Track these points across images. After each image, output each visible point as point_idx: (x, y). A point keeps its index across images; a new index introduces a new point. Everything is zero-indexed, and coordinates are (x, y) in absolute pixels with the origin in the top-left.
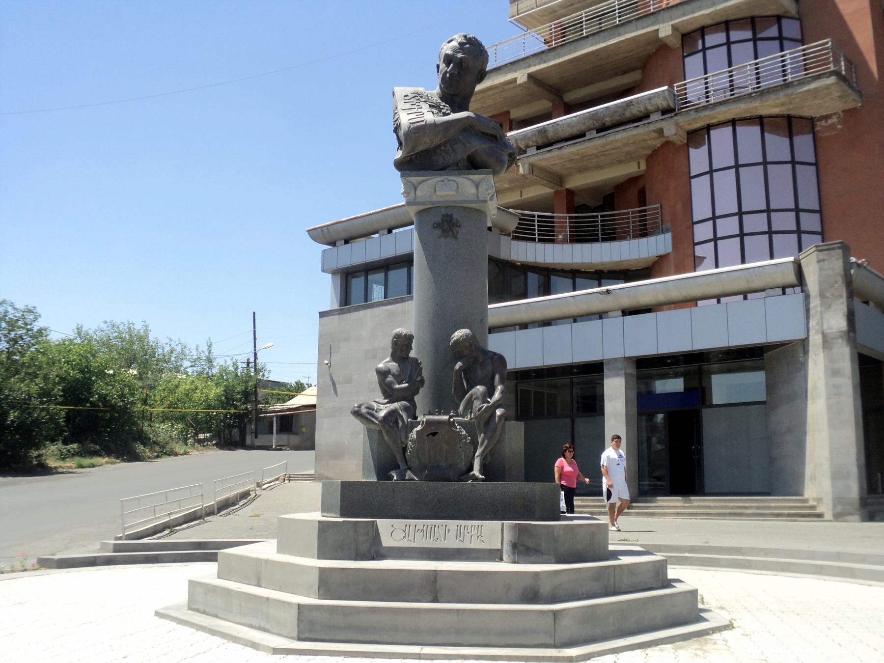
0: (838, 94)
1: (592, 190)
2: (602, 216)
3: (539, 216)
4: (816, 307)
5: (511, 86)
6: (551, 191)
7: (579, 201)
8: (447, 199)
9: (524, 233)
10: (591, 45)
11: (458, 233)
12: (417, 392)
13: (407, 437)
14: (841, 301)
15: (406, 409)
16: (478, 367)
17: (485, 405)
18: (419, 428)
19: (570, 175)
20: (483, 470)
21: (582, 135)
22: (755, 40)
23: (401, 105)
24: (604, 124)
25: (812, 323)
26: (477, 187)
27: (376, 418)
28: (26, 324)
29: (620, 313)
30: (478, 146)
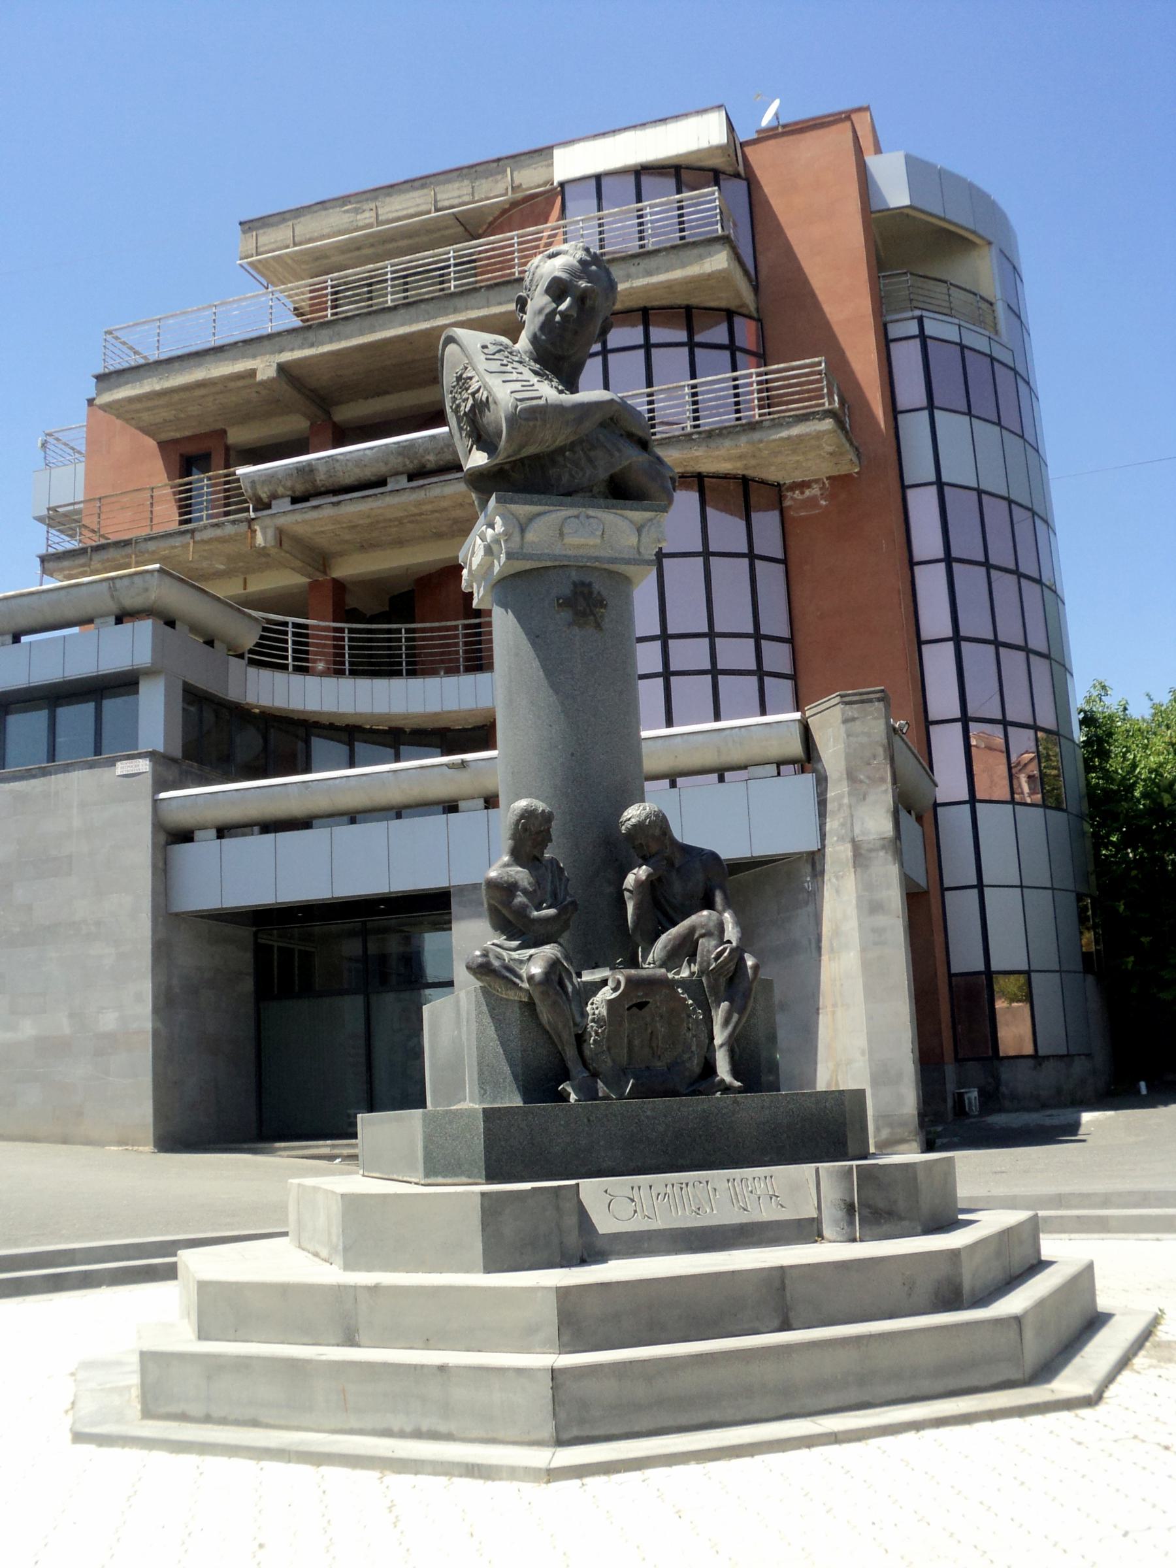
0: (830, 449)
1: (375, 584)
2: (408, 631)
3: (295, 625)
4: (841, 796)
5: (249, 381)
7: (351, 602)
8: (581, 552)
9: (267, 654)
11: (602, 617)
12: (565, 926)
13: (584, 1015)
14: (884, 787)
18: (606, 994)
19: (341, 554)
20: (736, 1073)
21: (381, 482)
22: (692, 345)
24: (424, 467)
25: (831, 825)
26: (639, 530)
27: (531, 978)
29: (481, 802)
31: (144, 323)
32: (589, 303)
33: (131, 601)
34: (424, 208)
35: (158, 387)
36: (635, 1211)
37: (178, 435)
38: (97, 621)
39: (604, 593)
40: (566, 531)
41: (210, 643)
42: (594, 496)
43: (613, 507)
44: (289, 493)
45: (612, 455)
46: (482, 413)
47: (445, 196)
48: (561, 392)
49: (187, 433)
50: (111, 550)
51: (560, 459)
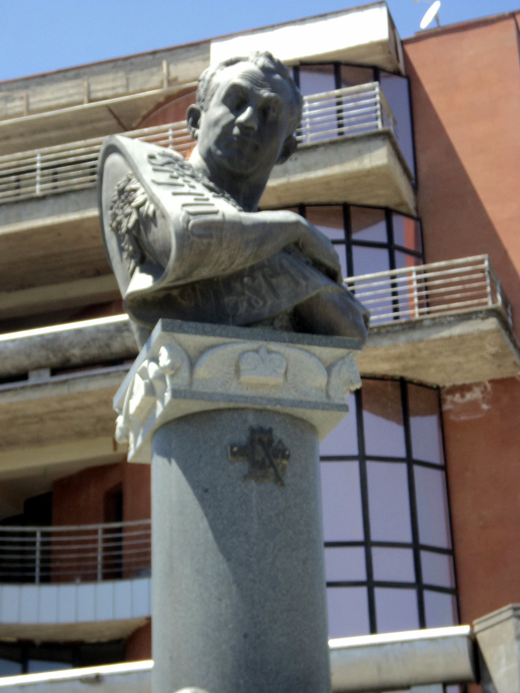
2: (44, 534)
8: (261, 392)
10: (51, 214)
11: (284, 468)
24: (68, 360)
26: (329, 369)
32: (272, 115)
34: (76, 98)
39: (287, 442)
40: (243, 367)
43: (298, 342)
45: (297, 284)
46: (147, 229)
47: (99, 87)
48: (240, 211)
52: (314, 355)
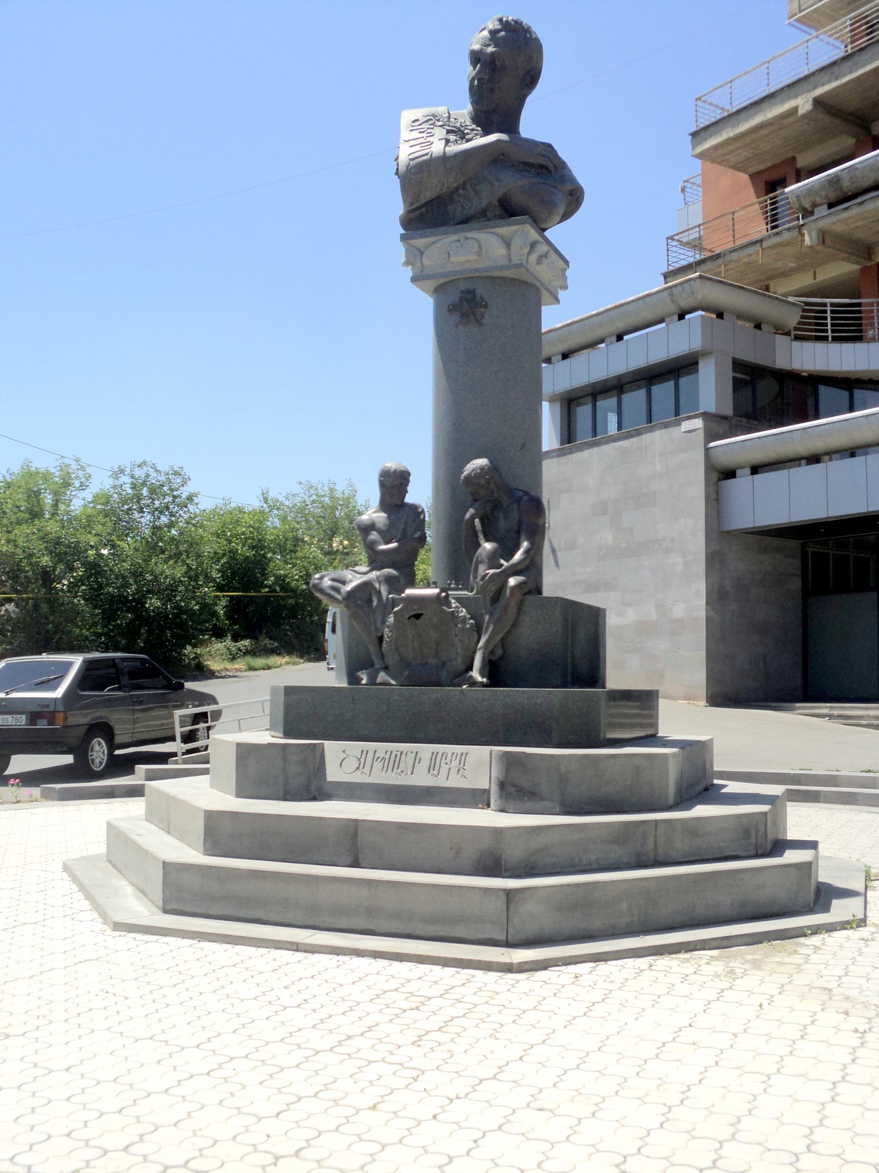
3: (832, 305)
5: (791, 120)
6: (857, 267)
8: (466, 266)
9: (812, 328)
11: (483, 315)
13: (384, 622)
15: (389, 581)
16: (501, 515)
17: (492, 571)
23: (405, 135)
28: (172, 490)
30: (510, 183)
31: (721, 86)
32: (498, 64)
33: (685, 304)
35: (731, 134)
36: (358, 768)
37: (762, 167)
38: (667, 320)
41: (758, 326)
42: (489, 219)
43: (486, 227)
44: (826, 201)
45: (492, 185)
49: (769, 165)
50: (708, 263)
51: (455, 197)
52: (497, 235)
